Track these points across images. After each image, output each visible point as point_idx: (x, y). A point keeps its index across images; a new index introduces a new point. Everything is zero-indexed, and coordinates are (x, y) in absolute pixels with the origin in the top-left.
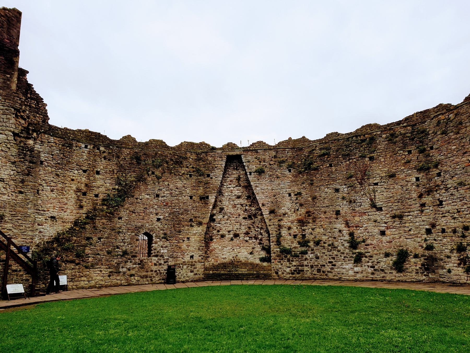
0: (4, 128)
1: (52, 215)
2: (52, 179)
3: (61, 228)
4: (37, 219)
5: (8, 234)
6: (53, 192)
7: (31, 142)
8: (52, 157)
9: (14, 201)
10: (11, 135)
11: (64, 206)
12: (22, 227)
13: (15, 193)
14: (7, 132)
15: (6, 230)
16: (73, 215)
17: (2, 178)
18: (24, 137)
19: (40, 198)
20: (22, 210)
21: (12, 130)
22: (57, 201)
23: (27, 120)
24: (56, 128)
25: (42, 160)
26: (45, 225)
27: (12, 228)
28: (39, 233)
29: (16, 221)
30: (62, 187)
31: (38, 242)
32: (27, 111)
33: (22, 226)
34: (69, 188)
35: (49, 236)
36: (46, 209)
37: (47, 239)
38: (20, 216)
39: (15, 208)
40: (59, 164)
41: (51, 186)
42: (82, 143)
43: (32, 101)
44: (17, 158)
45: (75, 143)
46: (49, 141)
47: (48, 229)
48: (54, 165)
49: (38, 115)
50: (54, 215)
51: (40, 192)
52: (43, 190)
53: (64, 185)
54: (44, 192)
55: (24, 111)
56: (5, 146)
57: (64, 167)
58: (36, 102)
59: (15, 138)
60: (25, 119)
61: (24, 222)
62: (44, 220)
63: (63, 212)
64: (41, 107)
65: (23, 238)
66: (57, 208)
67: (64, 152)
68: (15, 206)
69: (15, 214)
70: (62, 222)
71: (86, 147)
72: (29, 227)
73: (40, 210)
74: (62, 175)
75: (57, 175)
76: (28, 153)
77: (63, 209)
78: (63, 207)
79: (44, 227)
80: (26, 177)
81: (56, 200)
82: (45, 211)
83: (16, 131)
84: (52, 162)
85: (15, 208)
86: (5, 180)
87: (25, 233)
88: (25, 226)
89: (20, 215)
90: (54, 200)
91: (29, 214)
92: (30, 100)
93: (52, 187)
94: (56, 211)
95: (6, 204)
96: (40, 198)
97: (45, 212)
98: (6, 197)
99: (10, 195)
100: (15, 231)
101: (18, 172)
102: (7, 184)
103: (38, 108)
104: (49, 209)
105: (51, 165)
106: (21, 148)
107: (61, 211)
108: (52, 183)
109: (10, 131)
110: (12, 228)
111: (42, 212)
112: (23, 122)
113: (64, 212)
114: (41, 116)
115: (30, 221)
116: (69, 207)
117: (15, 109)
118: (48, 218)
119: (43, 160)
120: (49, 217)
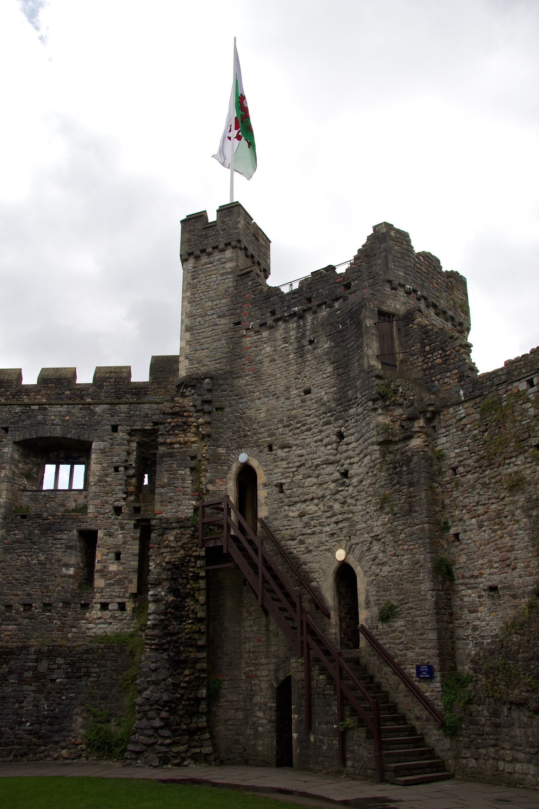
0: (366, 443)
1: (490, 584)
2: (476, 498)
3: (511, 613)
4: (465, 599)
5: (400, 641)
6: (483, 529)
7: (416, 442)
8: (469, 450)
9: (398, 573)
10: (375, 450)
11: (509, 554)
12: (417, 624)
13: (397, 556)
14: (371, 448)
15: (397, 633)
16: (531, 574)
17: (377, 534)
18: (400, 440)
19: (462, 550)
20: (412, 587)
21: (374, 439)
22: (492, 549)
23: (405, 402)
24: (495, 373)
25: (454, 465)
26: (480, 609)
27: (404, 628)
28: (472, 630)
29: (408, 612)
30: (499, 510)
31: (473, 652)
32: (400, 388)
33: (417, 621)
34: (511, 507)
35: (492, 636)
36: (476, 573)
37: (488, 644)
38: (412, 602)
39: (401, 587)
40: (483, 458)
41: (479, 516)
42: (519, 380)
43: (435, 354)
44: (388, 487)
45: (504, 390)
46: (458, 418)
47: (487, 619)
48: (476, 465)
49: (448, 374)
50: (494, 582)
51: (461, 536)
52: (465, 531)
53: (501, 503)
54: (468, 533)
55: (395, 392)
56: (371, 474)
57: (493, 462)
58: (440, 352)
59: (390, 450)
60: (401, 405)
61: (419, 613)
62: (477, 599)
63: (510, 571)
64: (451, 353)
65: (423, 648)
66: (496, 565)
67: (486, 425)
68: (401, 582)
69: (403, 599)
70: (511, 595)
71: (531, 383)
72: (427, 622)
73: (467, 578)
74: (493, 480)
75: (484, 485)
76: (405, 468)
77: (507, 562)
78: (509, 559)
79: (479, 614)
80: (408, 517)
81: (490, 545)
82: (476, 577)
83: (380, 439)
84: (470, 462)
85: (401, 587)
86: (380, 536)
87: (425, 636)
88: (422, 622)
89: (411, 599)
90: (488, 547)
91: (422, 593)
92: (430, 356)
93: (481, 517)
94: (496, 570)
95: (389, 582)
96: (462, 550)
97: (477, 581)
98: (386, 568)
99: (391, 563)
100: (409, 633)
101: (395, 514)
102: (384, 543)
103: (447, 360)
104: (482, 571)
105: (470, 469)
106: (391, 466)
107: (507, 569)
108: (480, 507)
109: (373, 444)
110: (404, 628)
111: (472, 581)
112: (398, 411)
113: (513, 570)
114: (456, 371)
115: (428, 608)
116: (520, 554)
117: (374, 401)
118: (483, 593)
119: (456, 463)
120: (484, 590)
